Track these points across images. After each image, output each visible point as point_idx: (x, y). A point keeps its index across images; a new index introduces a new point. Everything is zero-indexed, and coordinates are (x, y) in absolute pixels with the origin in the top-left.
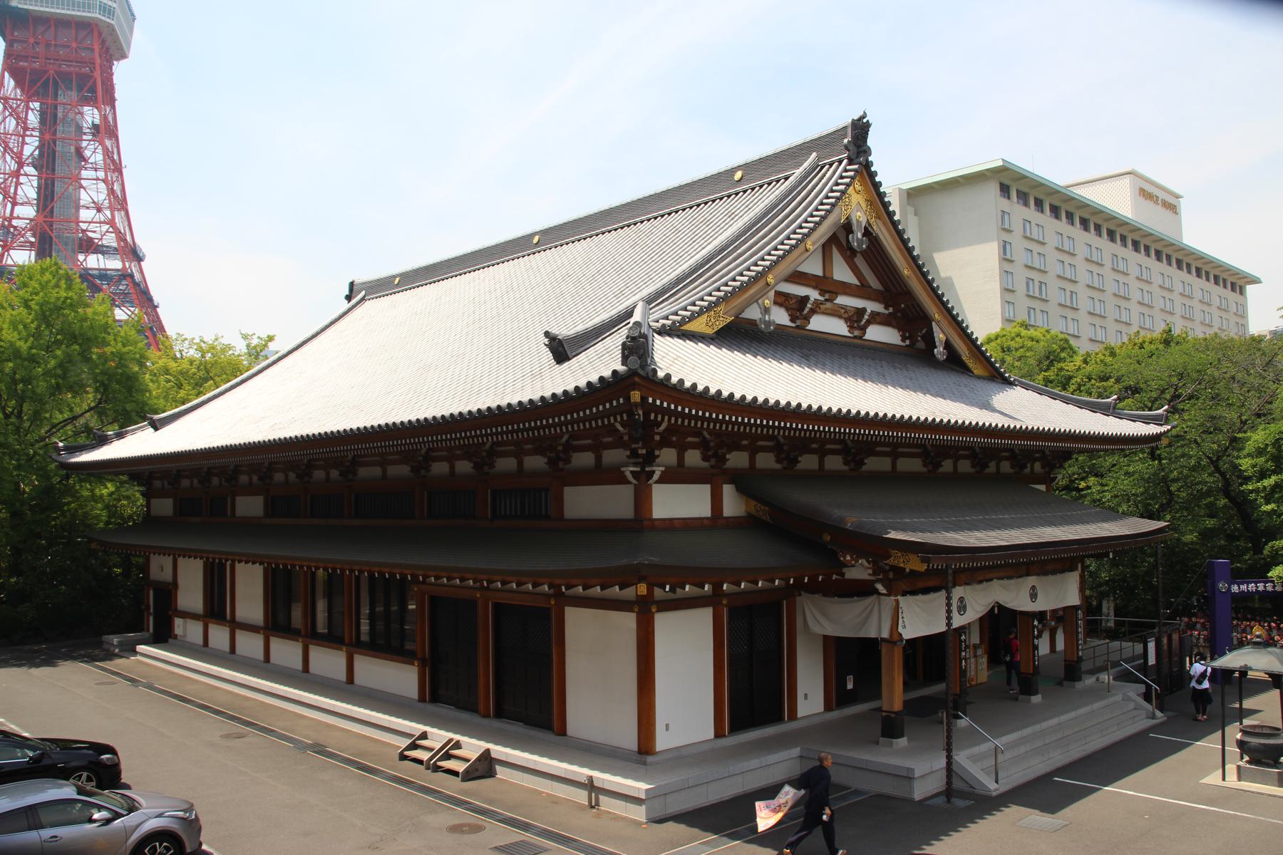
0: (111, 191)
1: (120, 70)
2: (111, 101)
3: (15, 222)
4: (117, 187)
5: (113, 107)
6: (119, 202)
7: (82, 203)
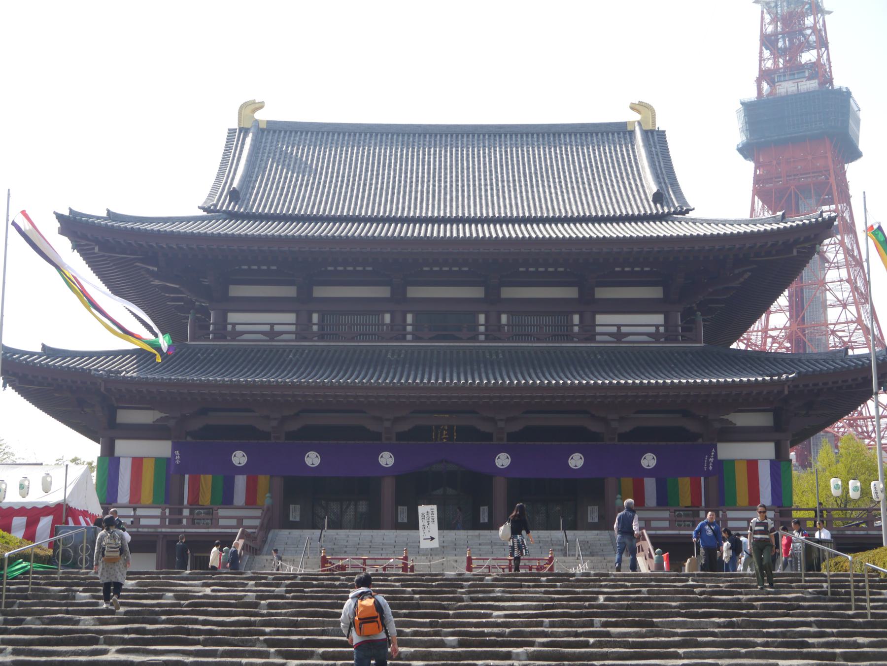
0: (855, 289)
1: (852, 170)
3: (770, 333)
4: (860, 284)
5: (849, 204)
7: (828, 303)
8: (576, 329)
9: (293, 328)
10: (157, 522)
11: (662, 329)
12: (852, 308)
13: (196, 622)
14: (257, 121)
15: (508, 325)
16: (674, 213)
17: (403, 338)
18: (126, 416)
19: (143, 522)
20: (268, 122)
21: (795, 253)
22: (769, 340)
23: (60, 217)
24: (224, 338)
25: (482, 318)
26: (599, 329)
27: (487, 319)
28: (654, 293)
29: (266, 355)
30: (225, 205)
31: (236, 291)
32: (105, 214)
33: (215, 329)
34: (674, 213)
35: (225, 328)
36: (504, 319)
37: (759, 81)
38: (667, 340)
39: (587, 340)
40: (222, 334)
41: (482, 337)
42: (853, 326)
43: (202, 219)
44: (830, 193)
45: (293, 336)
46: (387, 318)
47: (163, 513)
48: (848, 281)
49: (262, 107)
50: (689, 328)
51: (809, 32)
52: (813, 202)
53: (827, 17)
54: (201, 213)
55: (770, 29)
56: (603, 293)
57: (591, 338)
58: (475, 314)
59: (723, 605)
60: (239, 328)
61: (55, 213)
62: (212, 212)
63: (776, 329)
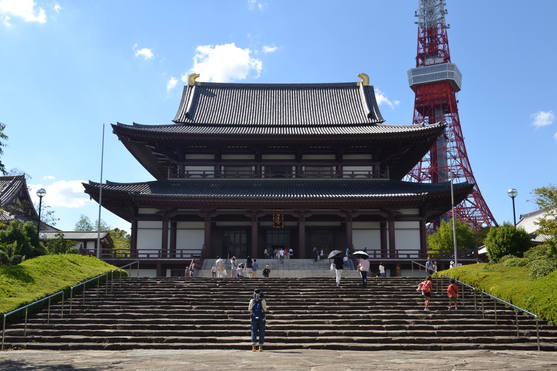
0: (460, 151)
2: (456, 110)
3: (422, 170)
4: (462, 149)
5: (457, 113)
6: (463, 155)
8: (334, 173)
9: (213, 173)
10: (157, 256)
11: (371, 173)
12: (458, 160)
13: (187, 297)
14: (196, 83)
15: (305, 171)
16: (377, 122)
17: (261, 177)
18: (143, 211)
19: (151, 256)
20: (202, 83)
21: (428, 140)
22: (422, 174)
23: (113, 126)
24: (184, 177)
25: (294, 168)
26: (344, 173)
27: (296, 169)
28: (368, 157)
29: (202, 185)
30: (184, 120)
31: (189, 157)
32: (132, 124)
33: (180, 173)
34: (377, 122)
35: (184, 173)
36: (304, 168)
37: (417, 58)
38: (374, 177)
39: (339, 177)
40: (183, 175)
41: (294, 176)
42: (459, 168)
43: (173, 126)
44: (449, 108)
45: (213, 176)
46: (254, 168)
47: (159, 252)
48: (457, 147)
49: (198, 76)
50: (383, 171)
51: (439, 36)
52: (441, 112)
53: (447, 30)
54: (173, 123)
55: (422, 35)
56: (346, 157)
57: (341, 177)
58: (291, 167)
59: (388, 290)
60: (190, 173)
61: (111, 124)
62: (178, 123)
63: (424, 169)
